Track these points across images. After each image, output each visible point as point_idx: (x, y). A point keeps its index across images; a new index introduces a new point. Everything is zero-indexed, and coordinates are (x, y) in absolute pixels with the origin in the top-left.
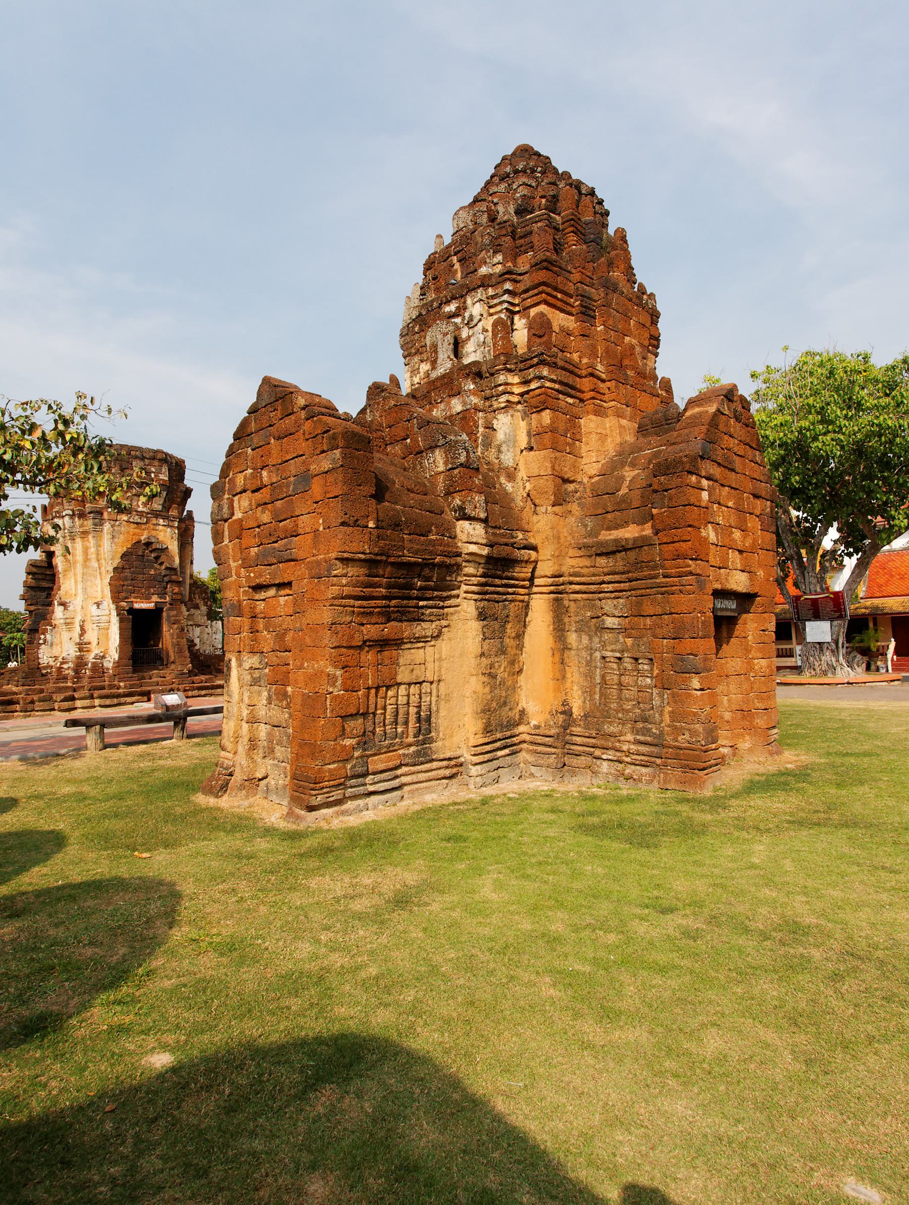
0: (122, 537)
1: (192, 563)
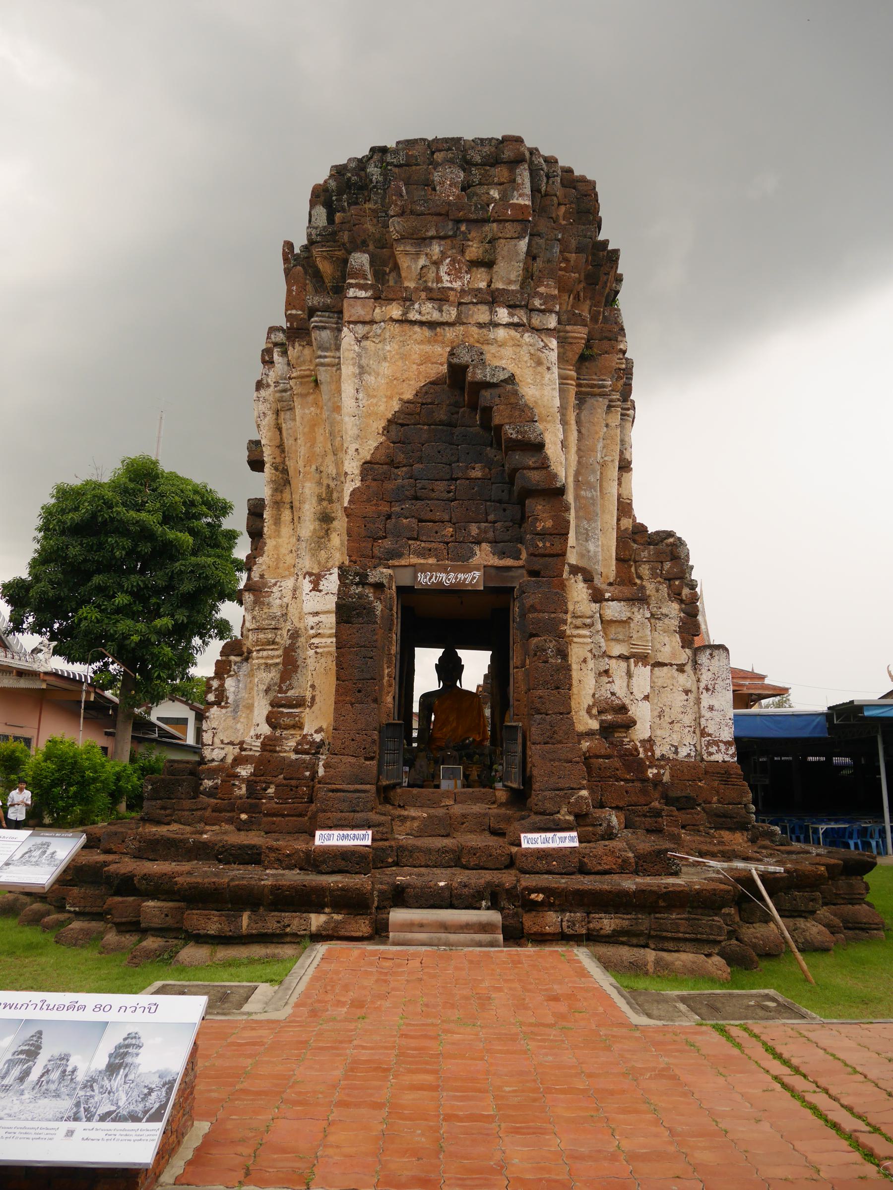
0: (385, 369)
1: (625, 466)
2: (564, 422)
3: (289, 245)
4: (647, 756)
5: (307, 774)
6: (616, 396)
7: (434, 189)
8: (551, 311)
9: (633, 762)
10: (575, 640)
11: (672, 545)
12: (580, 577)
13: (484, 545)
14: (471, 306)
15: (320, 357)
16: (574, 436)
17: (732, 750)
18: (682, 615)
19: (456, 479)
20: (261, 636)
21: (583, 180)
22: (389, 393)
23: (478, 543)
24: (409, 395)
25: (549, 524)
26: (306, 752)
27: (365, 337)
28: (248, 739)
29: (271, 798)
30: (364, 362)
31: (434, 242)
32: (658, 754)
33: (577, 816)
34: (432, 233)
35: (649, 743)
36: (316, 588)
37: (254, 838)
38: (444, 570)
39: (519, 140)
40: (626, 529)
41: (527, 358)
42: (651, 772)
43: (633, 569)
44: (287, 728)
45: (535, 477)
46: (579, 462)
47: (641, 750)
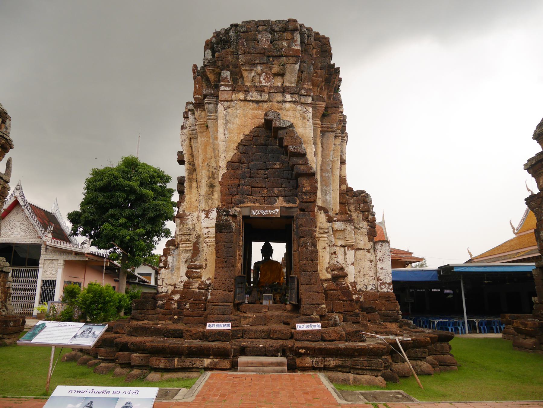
0: (237, 121)
1: (343, 162)
2: (315, 144)
3: (195, 66)
4: (353, 290)
5: (204, 298)
6: (339, 132)
7: (258, 42)
8: (309, 96)
9: (346, 292)
10: (321, 239)
11: (364, 196)
12: (322, 211)
13: (280, 198)
14: (274, 94)
15: (209, 116)
16: (320, 149)
17: (391, 287)
18: (369, 227)
19: (268, 169)
20: (183, 238)
21: (324, 37)
22: (238, 132)
23: (278, 197)
24: (247, 133)
25: (309, 188)
26: (203, 289)
27: (228, 107)
28: (178, 283)
29: (188, 309)
30: (228, 118)
31: (258, 65)
32: (358, 288)
33: (321, 316)
34: (257, 61)
35: (354, 284)
36: (207, 217)
37: (180, 326)
38: (263, 208)
39: (295, 21)
40: (344, 190)
41: (299, 116)
42: (355, 297)
43: (347, 207)
44: (195, 278)
45: (302, 168)
46: (322, 161)
47: (350, 287)
